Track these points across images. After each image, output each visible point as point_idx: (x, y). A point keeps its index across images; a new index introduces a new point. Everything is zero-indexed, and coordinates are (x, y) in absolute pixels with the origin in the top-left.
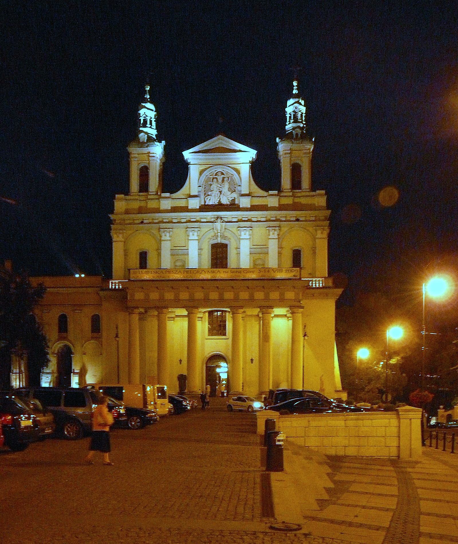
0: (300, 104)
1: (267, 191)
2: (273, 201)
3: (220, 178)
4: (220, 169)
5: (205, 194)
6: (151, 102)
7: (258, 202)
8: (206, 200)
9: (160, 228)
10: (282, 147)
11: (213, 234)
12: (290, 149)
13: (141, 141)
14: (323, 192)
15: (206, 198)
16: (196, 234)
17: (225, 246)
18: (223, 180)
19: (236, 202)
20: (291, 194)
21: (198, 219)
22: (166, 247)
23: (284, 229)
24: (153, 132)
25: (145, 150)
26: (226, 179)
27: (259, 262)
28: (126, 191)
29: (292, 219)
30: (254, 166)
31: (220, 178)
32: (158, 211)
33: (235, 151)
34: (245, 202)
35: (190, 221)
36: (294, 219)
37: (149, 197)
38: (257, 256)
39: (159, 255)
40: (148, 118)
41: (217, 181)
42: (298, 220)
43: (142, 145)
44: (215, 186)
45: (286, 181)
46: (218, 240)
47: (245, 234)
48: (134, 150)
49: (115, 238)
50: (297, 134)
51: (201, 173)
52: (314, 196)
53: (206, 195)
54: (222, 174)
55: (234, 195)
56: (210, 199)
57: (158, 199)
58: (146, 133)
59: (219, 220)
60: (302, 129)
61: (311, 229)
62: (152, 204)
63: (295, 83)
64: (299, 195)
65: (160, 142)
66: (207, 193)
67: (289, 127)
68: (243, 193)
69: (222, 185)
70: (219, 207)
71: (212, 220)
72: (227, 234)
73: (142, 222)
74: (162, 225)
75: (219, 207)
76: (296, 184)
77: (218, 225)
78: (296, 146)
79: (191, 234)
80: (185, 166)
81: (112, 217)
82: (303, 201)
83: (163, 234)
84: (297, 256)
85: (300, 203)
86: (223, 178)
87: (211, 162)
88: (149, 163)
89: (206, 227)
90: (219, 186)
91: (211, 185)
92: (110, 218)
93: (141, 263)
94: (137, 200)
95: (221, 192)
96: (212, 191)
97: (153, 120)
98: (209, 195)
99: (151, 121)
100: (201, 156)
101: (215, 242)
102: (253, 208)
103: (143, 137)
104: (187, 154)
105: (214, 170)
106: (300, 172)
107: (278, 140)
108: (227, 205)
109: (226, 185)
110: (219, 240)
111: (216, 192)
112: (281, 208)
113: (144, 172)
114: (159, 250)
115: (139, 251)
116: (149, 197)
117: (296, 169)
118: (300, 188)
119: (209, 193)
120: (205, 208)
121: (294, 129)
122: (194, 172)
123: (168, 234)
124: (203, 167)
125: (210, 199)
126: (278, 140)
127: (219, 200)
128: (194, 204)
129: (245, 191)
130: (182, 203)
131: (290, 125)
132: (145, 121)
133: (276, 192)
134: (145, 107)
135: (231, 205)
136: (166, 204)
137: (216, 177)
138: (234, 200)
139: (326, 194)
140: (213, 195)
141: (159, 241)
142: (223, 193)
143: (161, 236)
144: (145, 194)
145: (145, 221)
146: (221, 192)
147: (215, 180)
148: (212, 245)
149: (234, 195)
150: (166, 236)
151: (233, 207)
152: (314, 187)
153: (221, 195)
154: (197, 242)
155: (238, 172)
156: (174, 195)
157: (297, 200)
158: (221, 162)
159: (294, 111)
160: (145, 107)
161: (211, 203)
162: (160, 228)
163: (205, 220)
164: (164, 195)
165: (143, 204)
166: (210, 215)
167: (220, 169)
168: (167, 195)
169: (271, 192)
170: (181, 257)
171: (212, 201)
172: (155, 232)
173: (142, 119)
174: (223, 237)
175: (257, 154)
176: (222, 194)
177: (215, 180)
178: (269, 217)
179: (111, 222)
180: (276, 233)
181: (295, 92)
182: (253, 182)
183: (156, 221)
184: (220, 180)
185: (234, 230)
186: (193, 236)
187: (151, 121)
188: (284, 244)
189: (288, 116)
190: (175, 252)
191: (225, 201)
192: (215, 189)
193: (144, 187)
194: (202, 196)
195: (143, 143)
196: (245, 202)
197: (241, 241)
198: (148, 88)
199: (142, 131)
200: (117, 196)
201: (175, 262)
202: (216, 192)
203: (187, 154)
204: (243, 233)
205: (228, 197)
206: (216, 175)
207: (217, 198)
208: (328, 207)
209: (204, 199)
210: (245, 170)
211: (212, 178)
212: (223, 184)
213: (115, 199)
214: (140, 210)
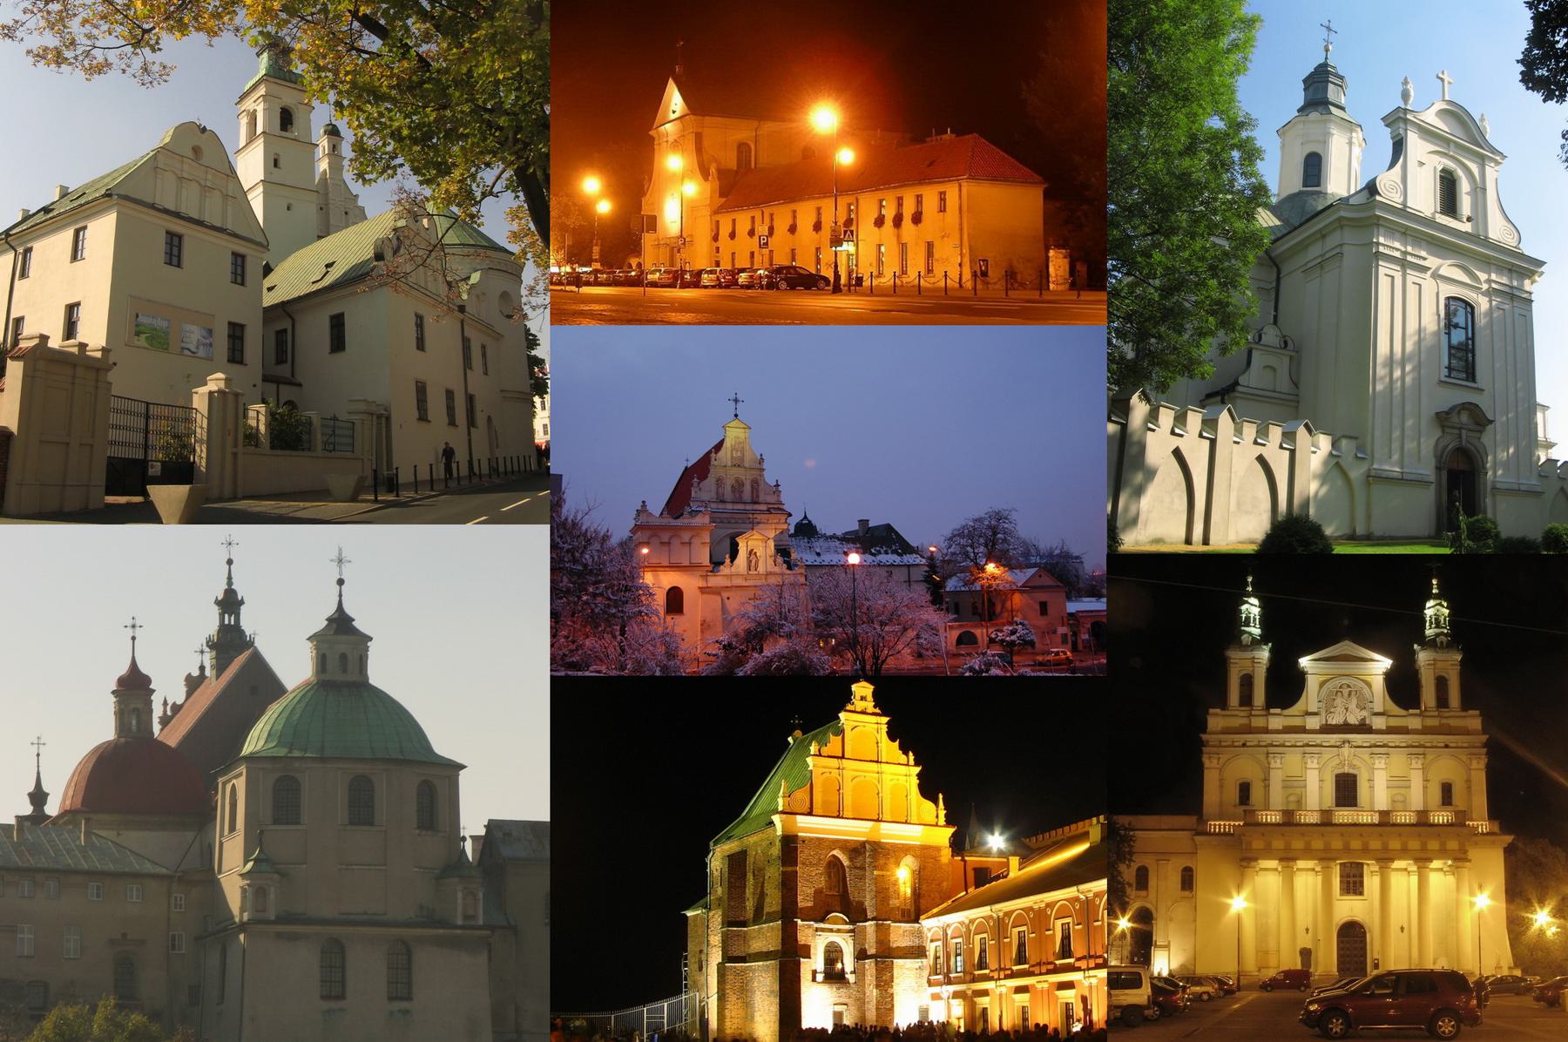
0: (1443, 606)
1: (1406, 708)
2: (1414, 723)
3: (1346, 691)
4: (1345, 681)
6: (1256, 597)
7: (1394, 722)
9: (1268, 753)
10: (1423, 657)
11: (1337, 761)
12: (1434, 660)
13: (1244, 643)
14: (1477, 712)
16: (1316, 761)
17: (1354, 777)
18: (1350, 695)
19: (1367, 722)
20: (1436, 713)
21: (1318, 742)
22: (1276, 778)
23: (1430, 757)
24: (1256, 631)
25: (1248, 655)
26: (1353, 693)
27: (1399, 798)
28: (1223, 704)
29: (1439, 745)
30: (1391, 678)
31: (1346, 691)
32: (1266, 731)
33: (1372, 660)
34: (1379, 723)
35: (1308, 745)
36: (1443, 745)
37: (1253, 713)
38: (1395, 791)
39: (1267, 787)
40: (1252, 616)
42: (1447, 746)
43: (1245, 648)
44: (1339, 701)
45: (1428, 695)
47: (1380, 763)
48: (1234, 655)
49: (1207, 762)
50: (1442, 642)
51: (1322, 684)
52: (1465, 717)
53: (1328, 712)
54: (1349, 686)
55: (1364, 713)
57: (1266, 715)
58: (1250, 634)
59: (1347, 745)
60: (1446, 635)
61: (1464, 758)
62: (1258, 722)
63: (1434, 582)
64: (1447, 715)
65: (1266, 644)
66: (1329, 706)
67: (1429, 632)
68: (1376, 710)
70: (1346, 728)
71: (1338, 744)
72: (1355, 762)
73: (1244, 745)
74: (1272, 749)
75: (1346, 728)
76: (1442, 702)
77: (1346, 750)
78: (1440, 656)
79: (1309, 761)
80: (1300, 678)
81: (1204, 737)
82: (1453, 722)
83: (1272, 761)
84: (1447, 791)
85: (1449, 725)
86: (1350, 692)
87: (1340, 672)
88: (1253, 671)
89: (1328, 754)
92: (1201, 738)
93: (1241, 797)
94: (1236, 716)
95: (1347, 709)
97: (1258, 617)
99: (1255, 619)
100: (1322, 664)
102: (1390, 730)
103: (1245, 639)
104: (1305, 662)
105: (1338, 682)
106: (1446, 685)
107: (1416, 646)
108: (1355, 725)
109: (1354, 701)
110: (1346, 770)
111: (1340, 709)
112: (1425, 731)
113: (1247, 681)
114: (1266, 780)
115: (1241, 781)
116: (1253, 713)
117: (1441, 683)
118: (1448, 707)
120: (1327, 729)
121: (1437, 635)
122: (1312, 683)
123: (1279, 761)
124: (1324, 678)
126: (1416, 646)
128: (1313, 723)
129: (1378, 708)
130: (1297, 722)
131: (1431, 631)
132: (1248, 618)
133: (1418, 711)
134: (1247, 602)
135: (1360, 725)
136: (1276, 722)
138: (1364, 719)
139: (1481, 715)
141: (1267, 771)
143: (1269, 763)
144: (1247, 708)
145: (1248, 744)
146: (1347, 709)
148: (1338, 776)
149: (1364, 713)
150: (1275, 763)
151: (1364, 728)
152: (1466, 704)
154: (1317, 771)
155: (1369, 685)
156: (1286, 712)
157: (1444, 721)
158: (1347, 672)
159: (1435, 615)
160: (1247, 602)
161: (1334, 723)
162: (1268, 753)
163: (1327, 744)
164: (1272, 711)
165: (1244, 721)
166: (1335, 738)
167: (1345, 681)
168: (1278, 711)
169: (1411, 711)
170: (1298, 791)
171: (1336, 720)
172: (1262, 757)
173: (1244, 616)
174: (1352, 766)
175: (1392, 665)
178: (1410, 742)
179: (1202, 744)
180: (1420, 762)
181: (1434, 591)
182: (1387, 697)
183: (1264, 744)
184: (1346, 695)
185: (1366, 757)
186: (1313, 763)
187: (1255, 619)
188: (1430, 776)
189: (1428, 619)
190: (1289, 784)
191: (1353, 720)
193: (1246, 700)
194: (1323, 714)
195: (1247, 646)
196: (1379, 723)
197: (1376, 772)
198: (1250, 579)
199: (1245, 632)
200: (1211, 711)
201: (1287, 798)
202: (1340, 709)
203: (1305, 662)
204: (1377, 761)
206: (1341, 687)
208: (1484, 731)
210: (1378, 683)
213: (1208, 713)
214: (1249, 730)
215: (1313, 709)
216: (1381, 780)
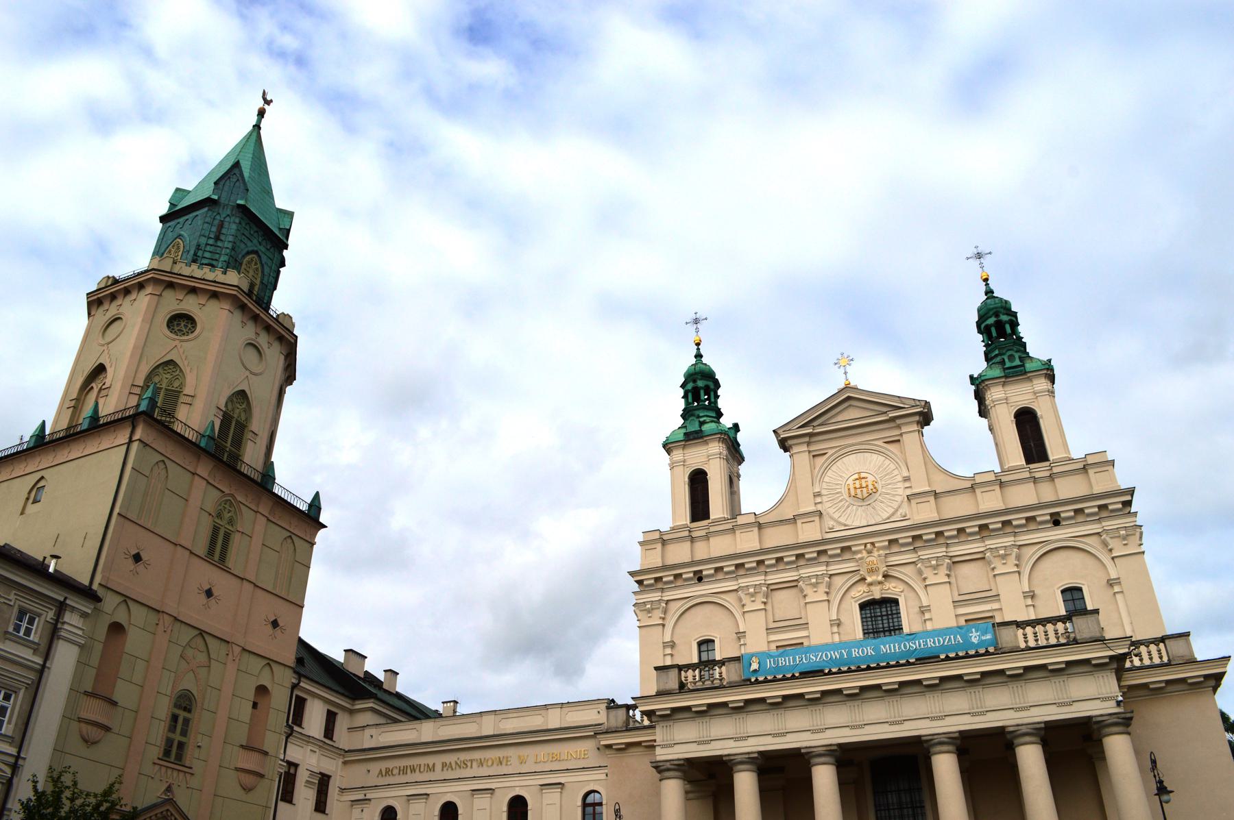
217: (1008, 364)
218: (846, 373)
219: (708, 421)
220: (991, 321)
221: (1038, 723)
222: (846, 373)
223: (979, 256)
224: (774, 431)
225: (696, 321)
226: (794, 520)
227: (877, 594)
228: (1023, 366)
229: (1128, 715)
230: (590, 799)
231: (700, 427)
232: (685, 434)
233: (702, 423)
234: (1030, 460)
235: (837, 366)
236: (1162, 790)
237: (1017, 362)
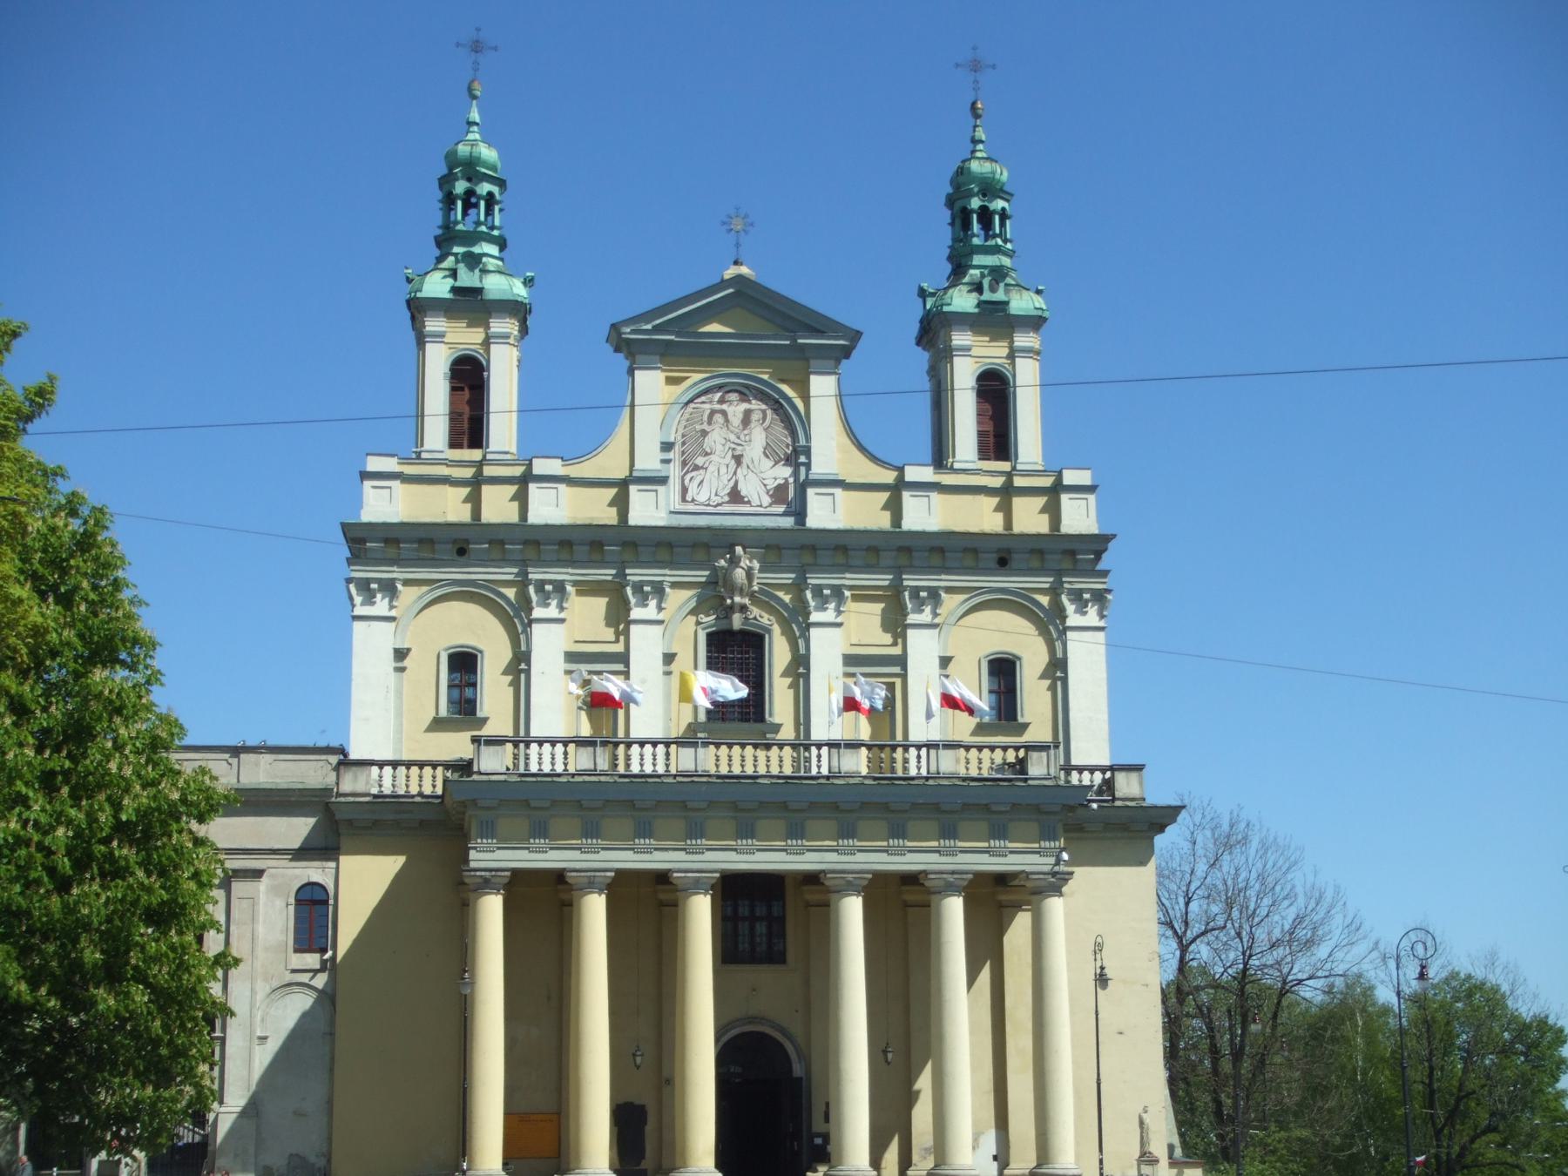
5: (684, 463)
8: (687, 482)
15: (688, 477)
18: (746, 420)
26: (756, 416)
41: (727, 420)
44: (717, 438)
46: (731, 624)
56: (702, 482)
69: (742, 437)
86: (747, 414)
90: (733, 437)
91: (704, 433)
95: (738, 459)
96: (711, 454)
98: (697, 468)
101: (723, 625)
109: (758, 437)
119: (700, 461)
125: (702, 482)
127: (732, 484)
137: (724, 407)
140: (711, 468)
142: (745, 460)
146: (738, 459)
147: (718, 418)
153: (739, 470)
161: (702, 498)
176: (744, 465)
177: (718, 418)
184: (736, 420)
192: (719, 448)
194: (674, 471)
205: (762, 475)
206: (721, 401)
207: (725, 478)
209: (683, 481)
211: (708, 412)
212: (746, 432)
215: (648, 460)
216: (827, 649)
217: (987, 296)
218: (738, 245)
219: (491, 268)
220: (975, 203)
221: (966, 873)
222: (738, 245)
223: (976, 66)
224: (613, 326)
225: (477, 47)
226: (623, 485)
227: (737, 621)
228: (1007, 303)
229: (1067, 877)
230: (306, 895)
231: (481, 281)
232: (454, 290)
233: (484, 271)
234: (984, 454)
235: (725, 227)
236: (1102, 980)
237: (1000, 296)
